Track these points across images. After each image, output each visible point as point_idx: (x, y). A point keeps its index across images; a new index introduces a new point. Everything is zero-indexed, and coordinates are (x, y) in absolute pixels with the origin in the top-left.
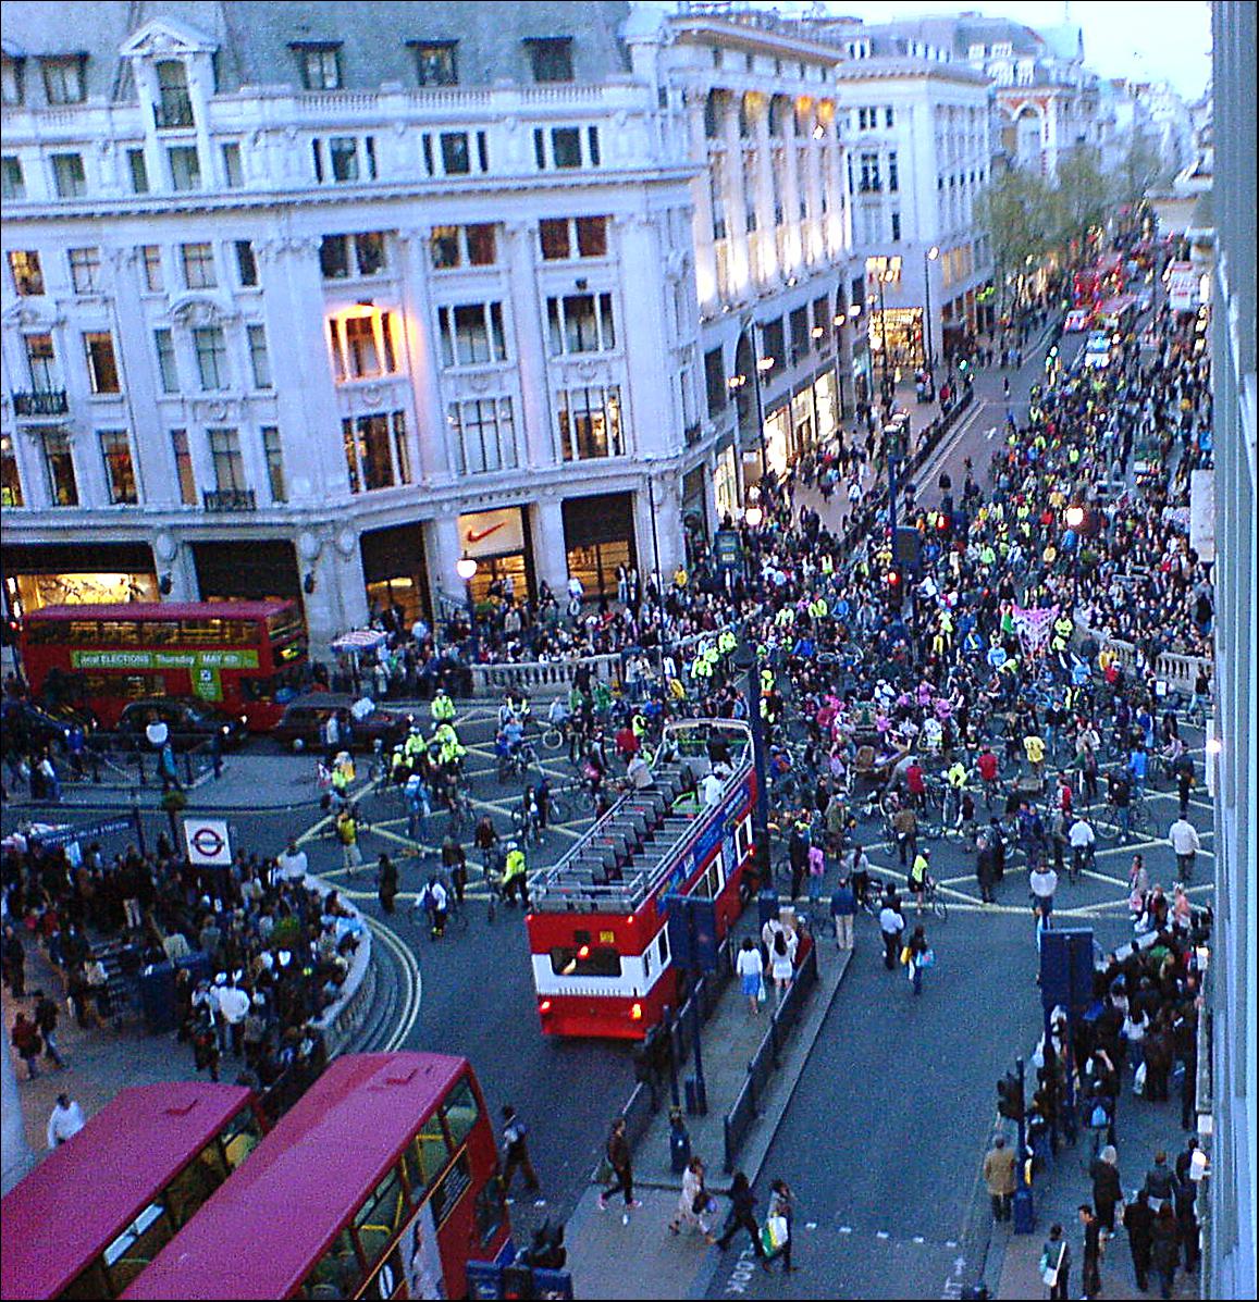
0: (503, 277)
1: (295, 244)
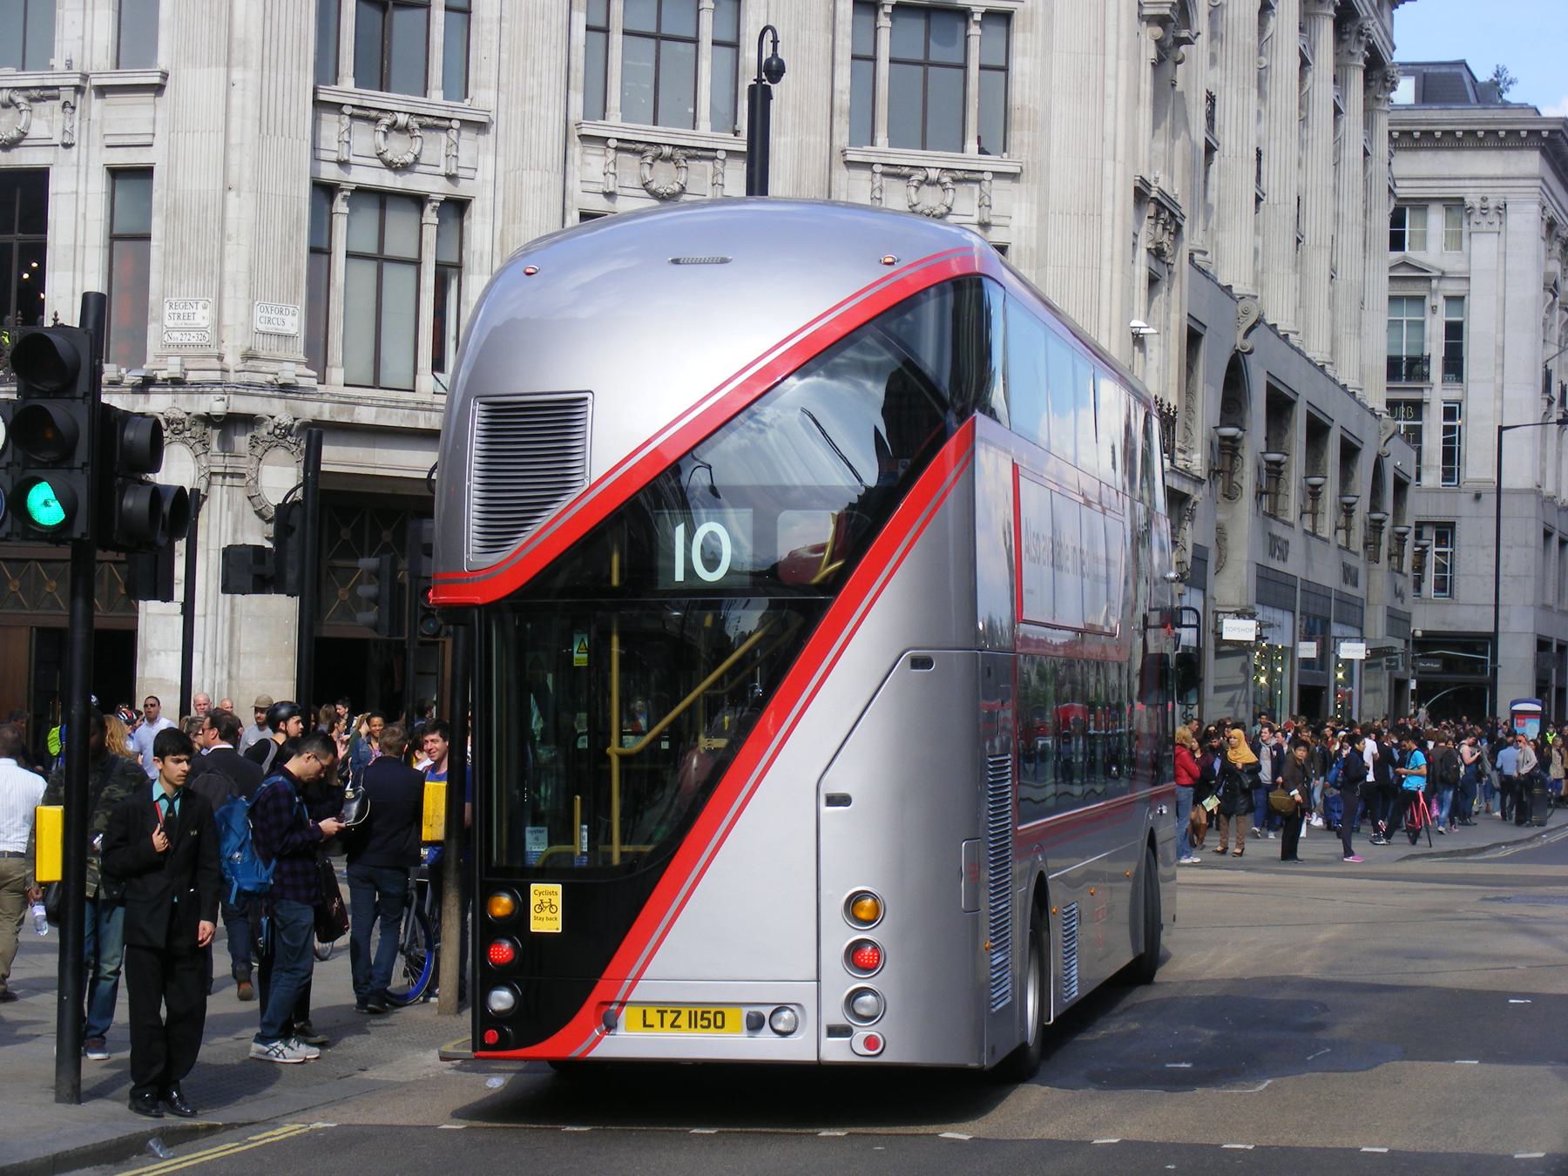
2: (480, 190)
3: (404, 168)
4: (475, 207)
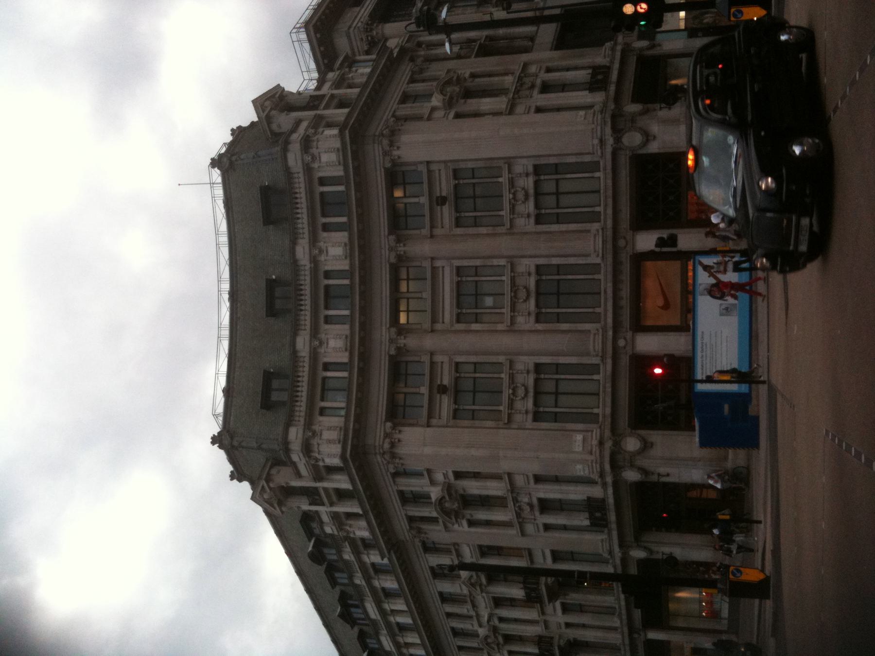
0: (438, 263)
1: (387, 446)
2: (531, 361)
4: (538, 361)
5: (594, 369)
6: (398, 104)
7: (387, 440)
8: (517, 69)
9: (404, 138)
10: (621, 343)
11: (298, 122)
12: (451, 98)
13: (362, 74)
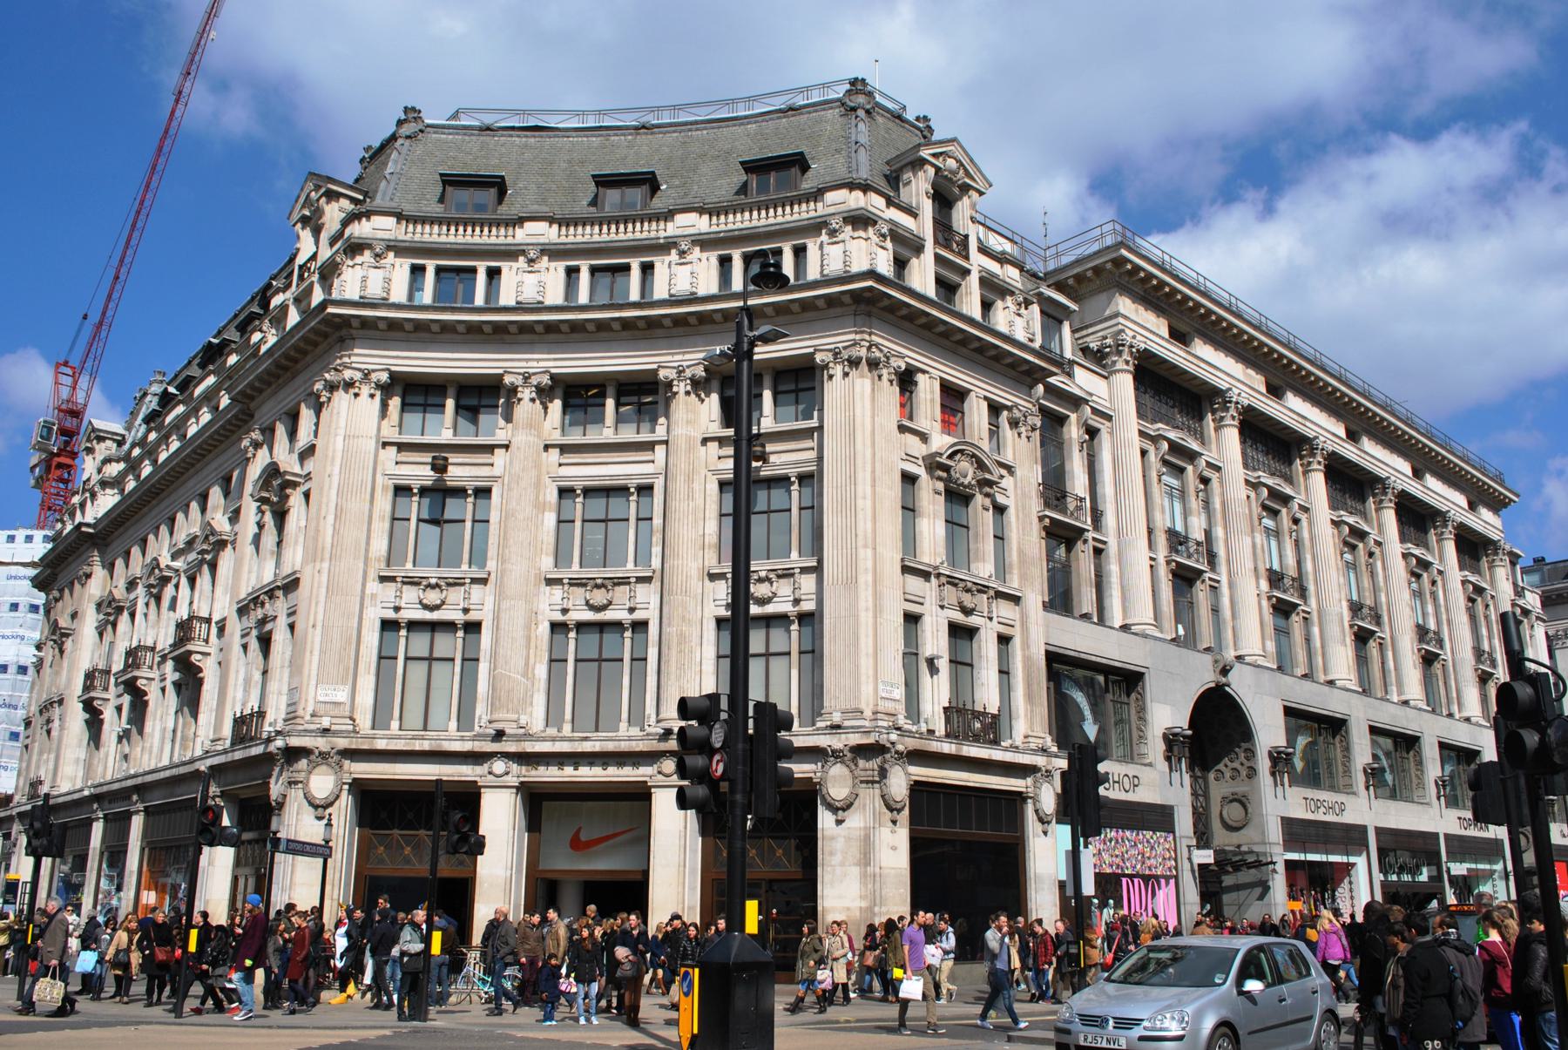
0: (660, 451)
1: (347, 374)
2: (484, 615)
3: (437, 608)
5: (465, 717)
6: (941, 378)
7: (358, 376)
8: (1013, 585)
9: (862, 382)
10: (499, 766)
11: (911, 212)
12: (947, 469)
13: (1011, 324)
